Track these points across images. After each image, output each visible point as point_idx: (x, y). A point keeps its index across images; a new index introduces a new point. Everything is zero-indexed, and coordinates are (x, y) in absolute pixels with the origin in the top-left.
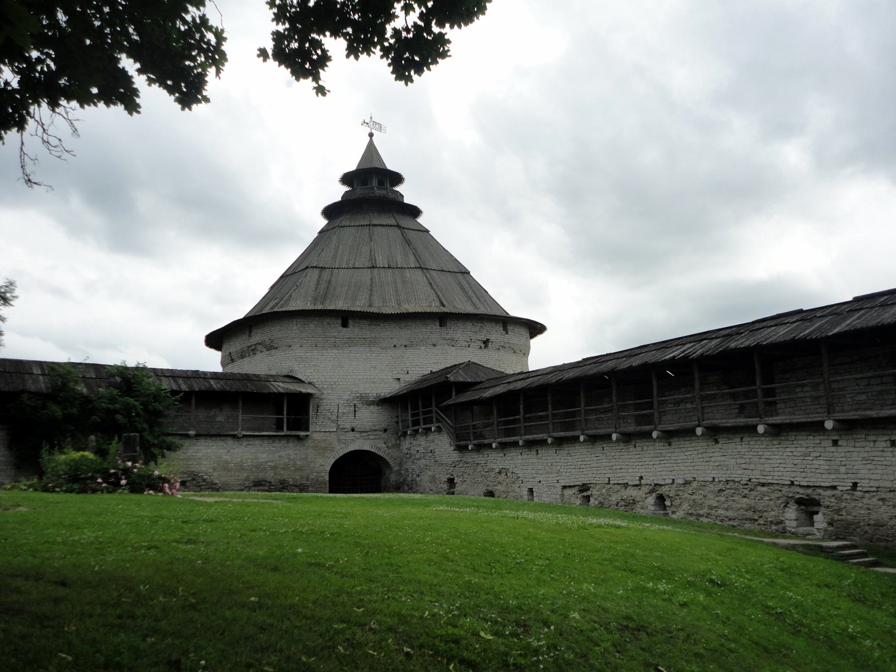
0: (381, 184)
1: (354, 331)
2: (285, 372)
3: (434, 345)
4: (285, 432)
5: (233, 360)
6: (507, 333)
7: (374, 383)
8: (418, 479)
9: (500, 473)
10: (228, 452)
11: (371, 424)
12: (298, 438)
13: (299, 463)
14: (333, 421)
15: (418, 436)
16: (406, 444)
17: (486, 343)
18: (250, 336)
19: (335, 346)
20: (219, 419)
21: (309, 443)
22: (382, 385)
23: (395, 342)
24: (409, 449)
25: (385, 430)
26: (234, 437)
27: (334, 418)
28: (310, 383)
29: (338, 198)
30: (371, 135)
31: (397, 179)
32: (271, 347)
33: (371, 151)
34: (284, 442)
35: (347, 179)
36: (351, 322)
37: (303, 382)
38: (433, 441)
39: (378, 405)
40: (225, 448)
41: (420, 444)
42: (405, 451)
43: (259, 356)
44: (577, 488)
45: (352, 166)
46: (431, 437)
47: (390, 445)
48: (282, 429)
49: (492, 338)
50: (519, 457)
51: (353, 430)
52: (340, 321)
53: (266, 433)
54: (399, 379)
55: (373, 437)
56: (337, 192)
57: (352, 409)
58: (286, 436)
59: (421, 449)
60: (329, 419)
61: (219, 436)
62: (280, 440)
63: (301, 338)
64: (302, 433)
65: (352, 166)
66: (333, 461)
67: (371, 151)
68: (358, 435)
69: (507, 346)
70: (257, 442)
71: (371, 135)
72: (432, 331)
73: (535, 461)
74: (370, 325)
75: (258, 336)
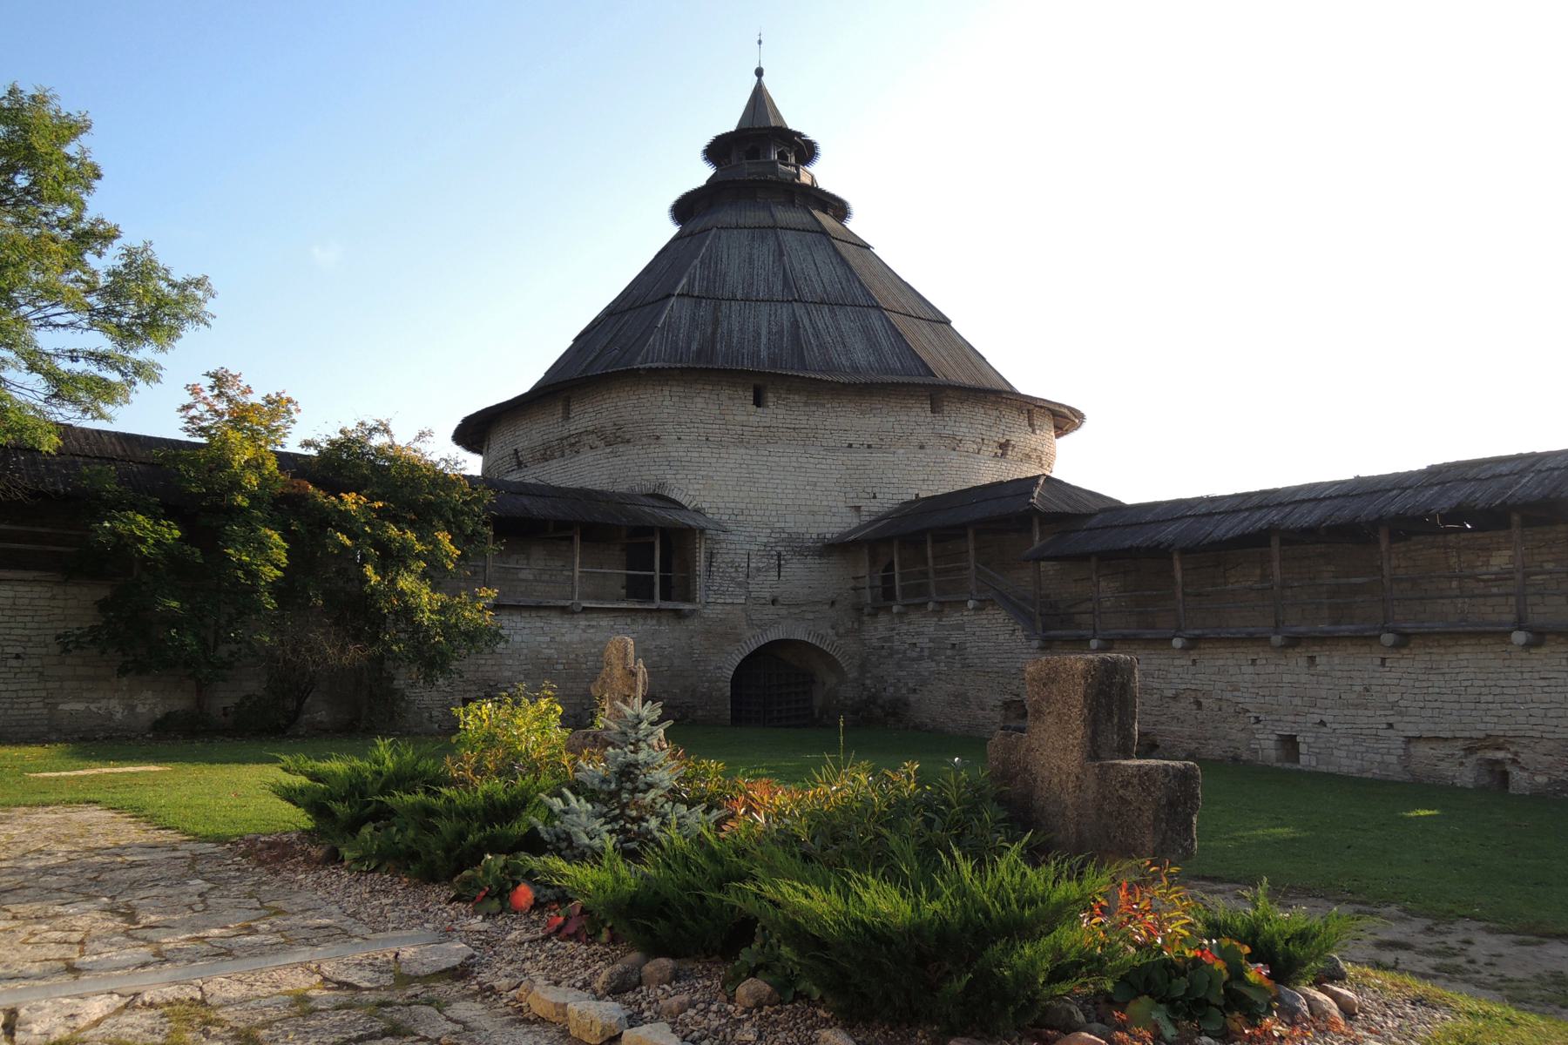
0: (783, 157)
1: (777, 413)
2: (649, 487)
3: (922, 447)
4: (658, 603)
5: (520, 464)
6: (1034, 432)
7: (813, 513)
8: (912, 698)
9: (1175, 698)
10: (553, 640)
11: (807, 591)
12: (679, 615)
13: (677, 662)
14: (739, 584)
15: (914, 617)
16: (878, 629)
17: (1004, 446)
18: (566, 417)
19: (741, 441)
20: (523, 575)
21: (693, 624)
22: (827, 519)
23: (852, 438)
24: (889, 639)
25: (833, 603)
26: (564, 610)
27: (742, 577)
28: (698, 511)
29: (701, 182)
30: (759, 72)
31: (806, 151)
32: (615, 438)
33: (759, 100)
34: (651, 624)
35: (717, 151)
36: (770, 397)
37: (683, 507)
38: (961, 627)
39: (820, 556)
40: (545, 634)
41: (922, 629)
42: (876, 643)
43: (587, 457)
44: (1460, 743)
45: (729, 122)
46: (954, 618)
47: (841, 631)
48: (651, 598)
49: (1014, 439)
50: (1251, 669)
51: (774, 602)
52: (750, 395)
53: (624, 605)
54: (858, 508)
55: (811, 616)
56: (700, 174)
57: (774, 561)
58: (659, 610)
59: (923, 642)
60: (733, 579)
61: (538, 608)
62: (645, 618)
63: (679, 424)
64: (687, 607)
65: (730, 125)
66: (738, 659)
67: (759, 100)
68: (784, 612)
69: (1034, 455)
70: (605, 622)
71: (759, 72)
72: (915, 419)
73: (1304, 678)
74: (806, 404)
75: (587, 416)
